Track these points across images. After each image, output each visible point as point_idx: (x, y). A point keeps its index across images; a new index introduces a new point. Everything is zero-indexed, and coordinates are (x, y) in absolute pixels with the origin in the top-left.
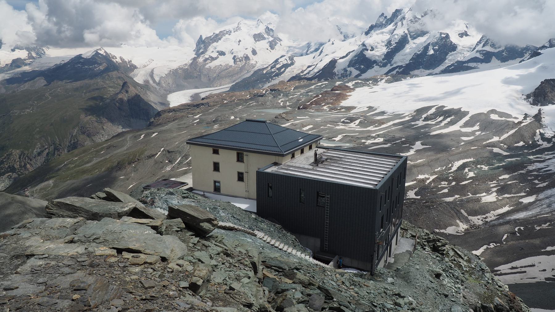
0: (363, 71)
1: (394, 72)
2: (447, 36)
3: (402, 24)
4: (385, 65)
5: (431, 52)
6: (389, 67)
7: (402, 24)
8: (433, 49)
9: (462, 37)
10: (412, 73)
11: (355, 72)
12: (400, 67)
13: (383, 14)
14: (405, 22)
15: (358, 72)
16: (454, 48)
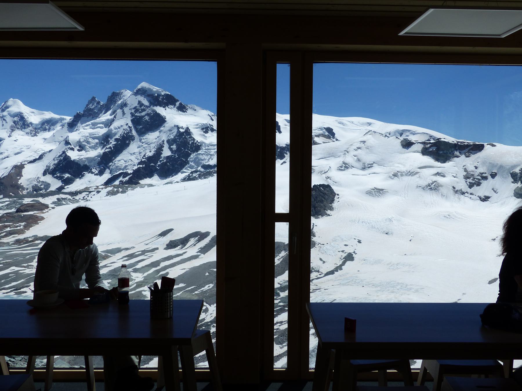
0: (68, 182)
1: (117, 183)
2: (187, 132)
3: (124, 114)
4: (101, 173)
5: (166, 152)
6: (107, 176)
7: (124, 114)
8: (171, 149)
9: (206, 132)
10: (142, 182)
11: (55, 184)
12: (125, 174)
13: (93, 99)
14: (126, 110)
15: (59, 184)
16: (197, 147)
